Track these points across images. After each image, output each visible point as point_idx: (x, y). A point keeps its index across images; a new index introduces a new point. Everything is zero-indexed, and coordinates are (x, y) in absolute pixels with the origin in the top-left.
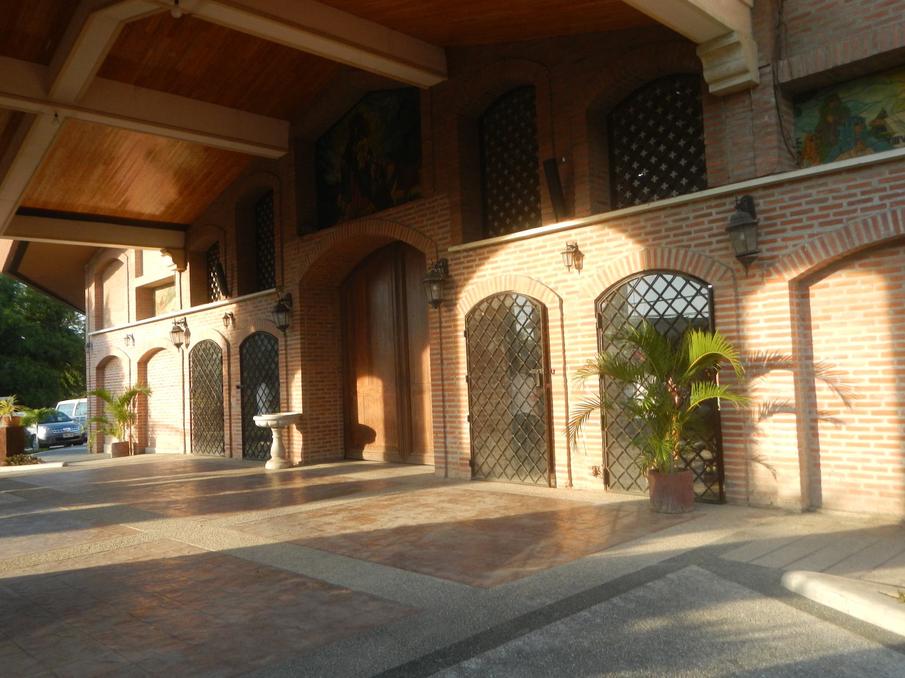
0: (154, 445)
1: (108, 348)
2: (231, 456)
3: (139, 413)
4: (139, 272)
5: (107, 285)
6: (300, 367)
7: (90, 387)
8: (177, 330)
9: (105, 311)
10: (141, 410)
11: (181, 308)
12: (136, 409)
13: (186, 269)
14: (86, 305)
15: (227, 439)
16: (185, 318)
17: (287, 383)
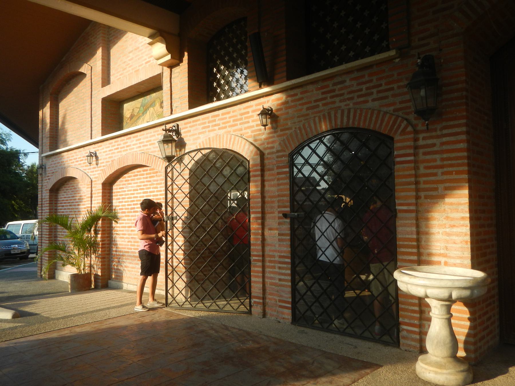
0: (120, 277)
1: (64, 169)
2: (264, 315)
3: (102, 241)
4: (106, 81)
5: (63, 105)
6: (467, 185)
7: (42, 210)
8: (167, 140)
9: (60, 132)
10: (104, 237)
11: (171, 113)
12: (99, 236)
13: (181, 61)
14: (40, 126)
15: (256, 288)
16: (178, 125)
17: (417, 211)
